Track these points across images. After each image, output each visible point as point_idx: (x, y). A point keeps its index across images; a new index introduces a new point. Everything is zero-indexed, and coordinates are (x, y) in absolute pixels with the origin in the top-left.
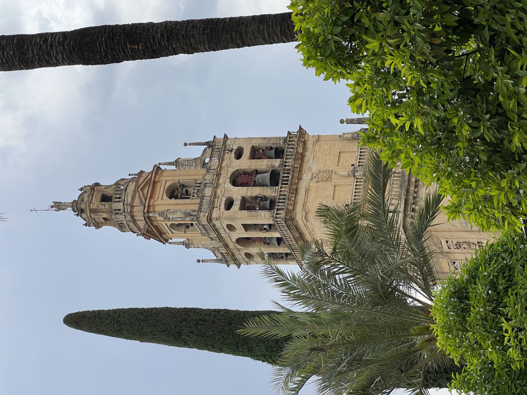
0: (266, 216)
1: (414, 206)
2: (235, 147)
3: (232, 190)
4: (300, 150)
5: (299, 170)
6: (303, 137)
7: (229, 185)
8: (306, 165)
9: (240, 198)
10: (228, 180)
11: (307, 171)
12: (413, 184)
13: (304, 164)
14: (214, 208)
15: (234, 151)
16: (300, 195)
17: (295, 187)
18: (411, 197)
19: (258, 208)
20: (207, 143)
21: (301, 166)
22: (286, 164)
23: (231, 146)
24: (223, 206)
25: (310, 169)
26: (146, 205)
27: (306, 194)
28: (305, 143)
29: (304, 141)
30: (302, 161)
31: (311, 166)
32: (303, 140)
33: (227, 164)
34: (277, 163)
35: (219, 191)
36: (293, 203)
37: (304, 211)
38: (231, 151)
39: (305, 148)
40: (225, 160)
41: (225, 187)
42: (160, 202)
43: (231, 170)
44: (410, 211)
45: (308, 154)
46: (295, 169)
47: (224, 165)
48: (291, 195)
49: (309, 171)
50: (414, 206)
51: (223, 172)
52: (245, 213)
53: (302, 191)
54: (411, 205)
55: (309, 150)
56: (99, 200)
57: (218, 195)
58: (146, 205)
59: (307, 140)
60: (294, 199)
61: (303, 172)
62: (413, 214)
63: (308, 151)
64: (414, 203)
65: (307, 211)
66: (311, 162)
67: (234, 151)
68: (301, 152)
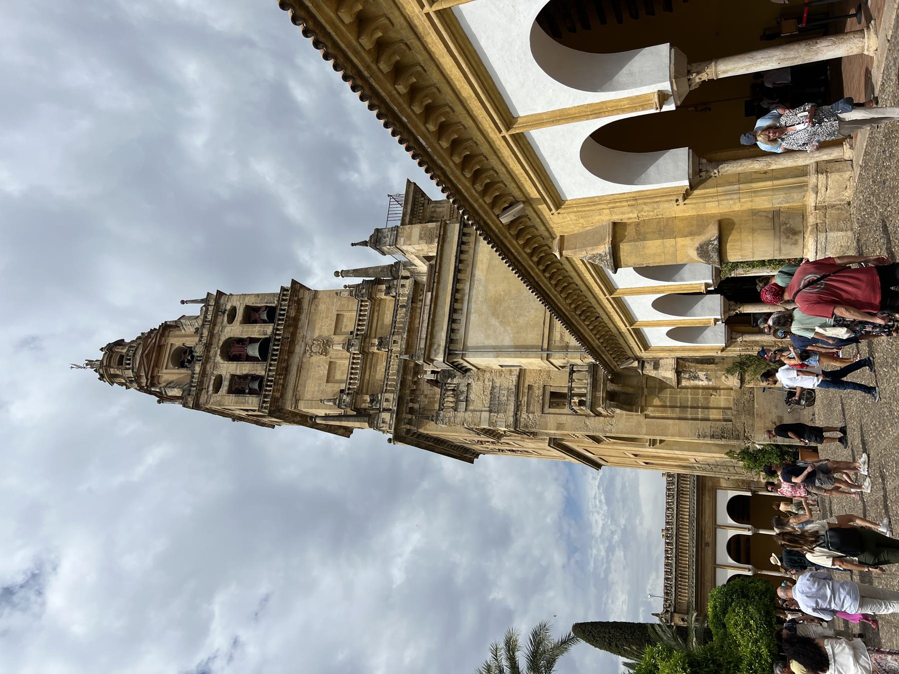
0: (254, 402)
1: (411, 405)
2: (228, 307)
3: (222, 365)
4: (293, 314)
5: (290, 342)
6: (296, 294)
7: (218, 358)
8: (300, 333)
9: (228, 376)
10: (219, 352)
11: (301, 342)
12: (411, 371)
13: (298, 331)
14: (202, 389)
15: (227, 312)
16: (291, 375)
17: (284, 365)
18: (408, 392)
19: (247, 391)
20: (202, 301)
21: (294, 334)
22: (278, 332)
23: (224, 306)
24: (211, 388)
25: (304, 337)
26: (149, 377)
27: (297, 373)
28: (299, 303)
29: (299, 299)
30: (296, 327)
31: (305, 334)
32: (296, 299)
33: (219, 330)
34: (269, 329)
35: (208, 367)
36: (281, 388)
37: (294, 398)
38: (224, 313)
39: (299, 310)
40: (218, 325)
41: (216, 361)
42: (165, 371)
43: (223, 339)
44: (406, 413)
45: (303, 317)
46: (285, 340)
47: (215, 332)
48: (278, 377)
49: (303, 341)
50: (411, 405)
51: (215, 341)
52: (232, 398)
53: (294, 369)
54: (407, 403)
55: (304, 311)
56: (117, 363)
57: (207, 373)
58: (149, 377)
59: (302, 298)
60: (281, 382)
61: (296, 342)
62: (410, 416)
63: (303, 312)
64: (412, 401)
65: (298, 397)
66: (306, 329)
67: (227, 312)
68: (293, 315)
